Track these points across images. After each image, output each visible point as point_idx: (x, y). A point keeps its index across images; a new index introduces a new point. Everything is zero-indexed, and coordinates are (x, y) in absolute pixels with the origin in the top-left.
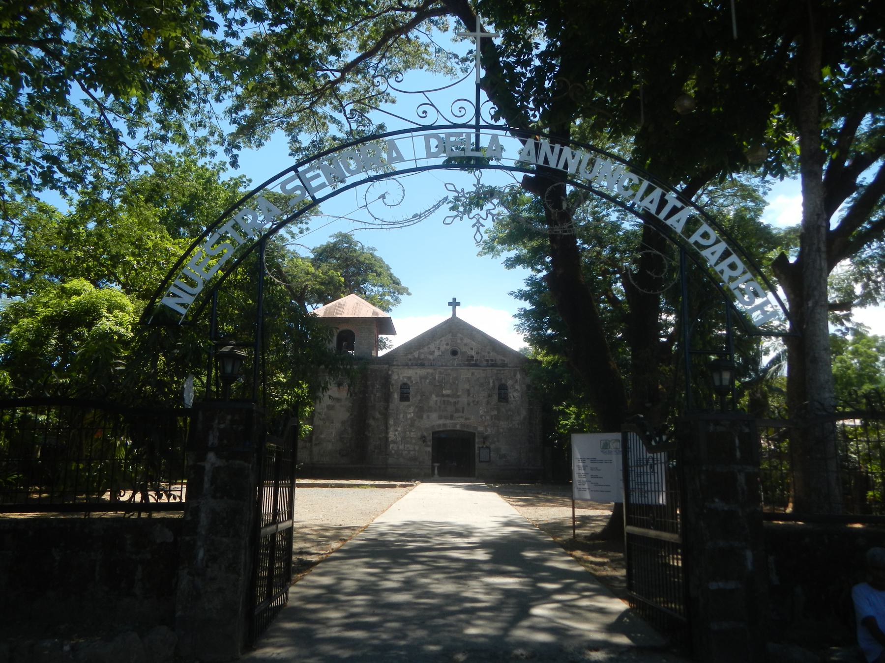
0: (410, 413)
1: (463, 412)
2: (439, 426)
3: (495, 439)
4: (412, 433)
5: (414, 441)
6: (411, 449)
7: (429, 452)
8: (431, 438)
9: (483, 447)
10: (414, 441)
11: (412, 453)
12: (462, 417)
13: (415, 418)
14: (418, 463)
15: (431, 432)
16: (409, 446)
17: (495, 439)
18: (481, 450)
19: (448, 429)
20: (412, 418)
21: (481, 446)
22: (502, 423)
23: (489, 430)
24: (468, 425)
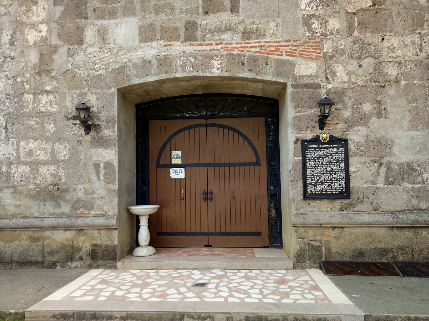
0: (33, 26)
1: (234, 9)
2: (147, 63)
3: (367, 107)
4: (44, 99)
5: (50, 127)
6: (43, 156)
7: (108, 165)
8: (114, 112)
9: (316, 140)
10: (50, 127)
11: (44, 170)
12: (228, 29)
13: (54, 41)
14: (66, 209)
15: (114, 90)
16: (32, 145)
17: (367, 107)
18: (311, 153)
19: (178, 75)
20: (44, 40)
21: (309, 136)
22: (395, 41)
23: (340, 70)
24: (255, 59)
